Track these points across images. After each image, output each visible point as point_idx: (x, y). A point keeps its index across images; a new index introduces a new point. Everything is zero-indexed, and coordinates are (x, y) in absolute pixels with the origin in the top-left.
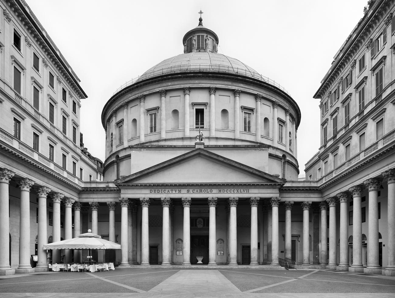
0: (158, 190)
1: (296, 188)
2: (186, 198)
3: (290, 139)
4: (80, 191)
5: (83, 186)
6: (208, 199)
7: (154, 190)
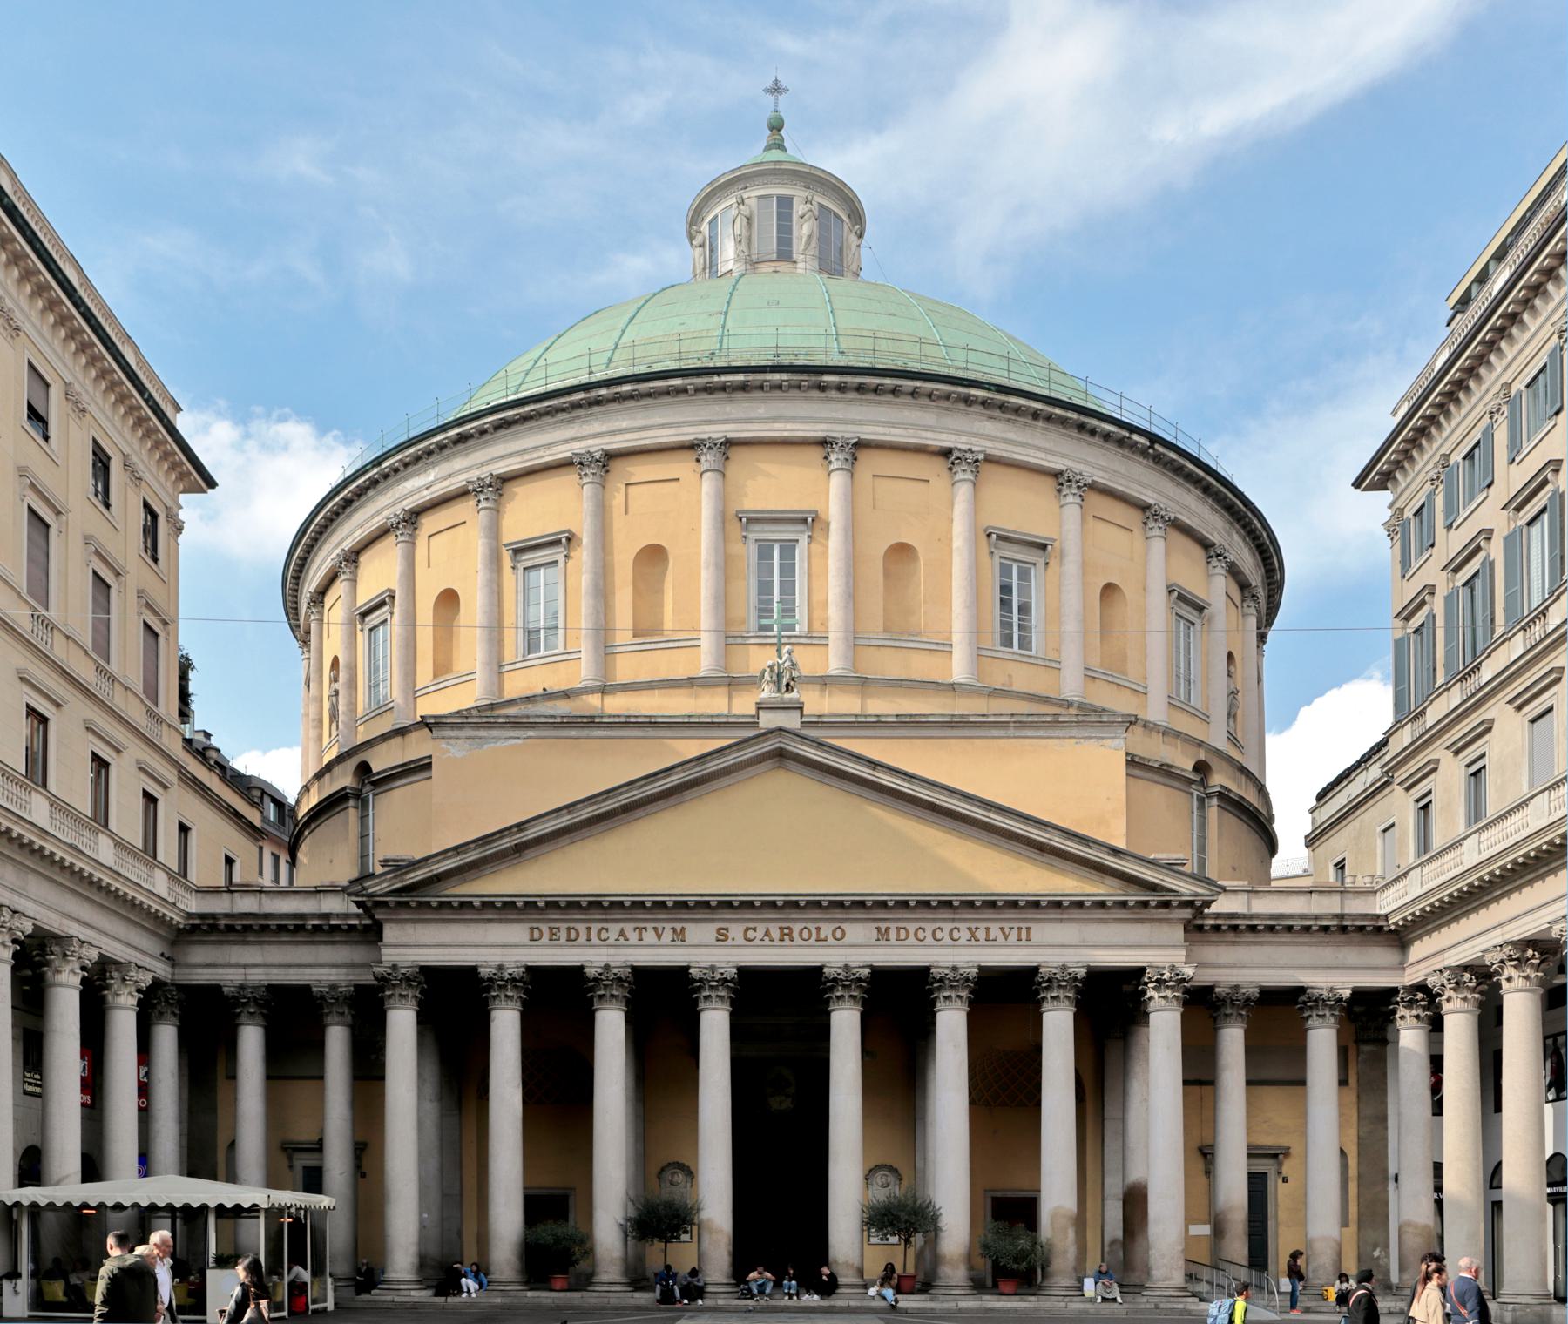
2: (713, 968)
3: (1232, 688)
4: (179, 929)
5: (193, 910)
6: (826, 970)
7: (551, 929)
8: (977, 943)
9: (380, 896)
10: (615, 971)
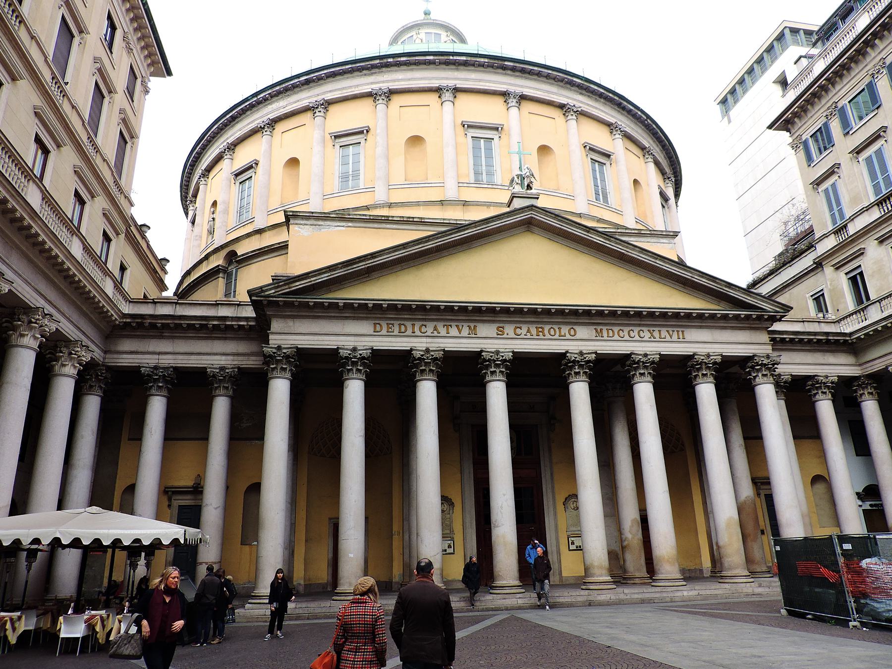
0: (399, 325)
1: (792, 337)
2: (497, 352)
8: (654, 340)
9: (272, 297)
10: (432, 353)
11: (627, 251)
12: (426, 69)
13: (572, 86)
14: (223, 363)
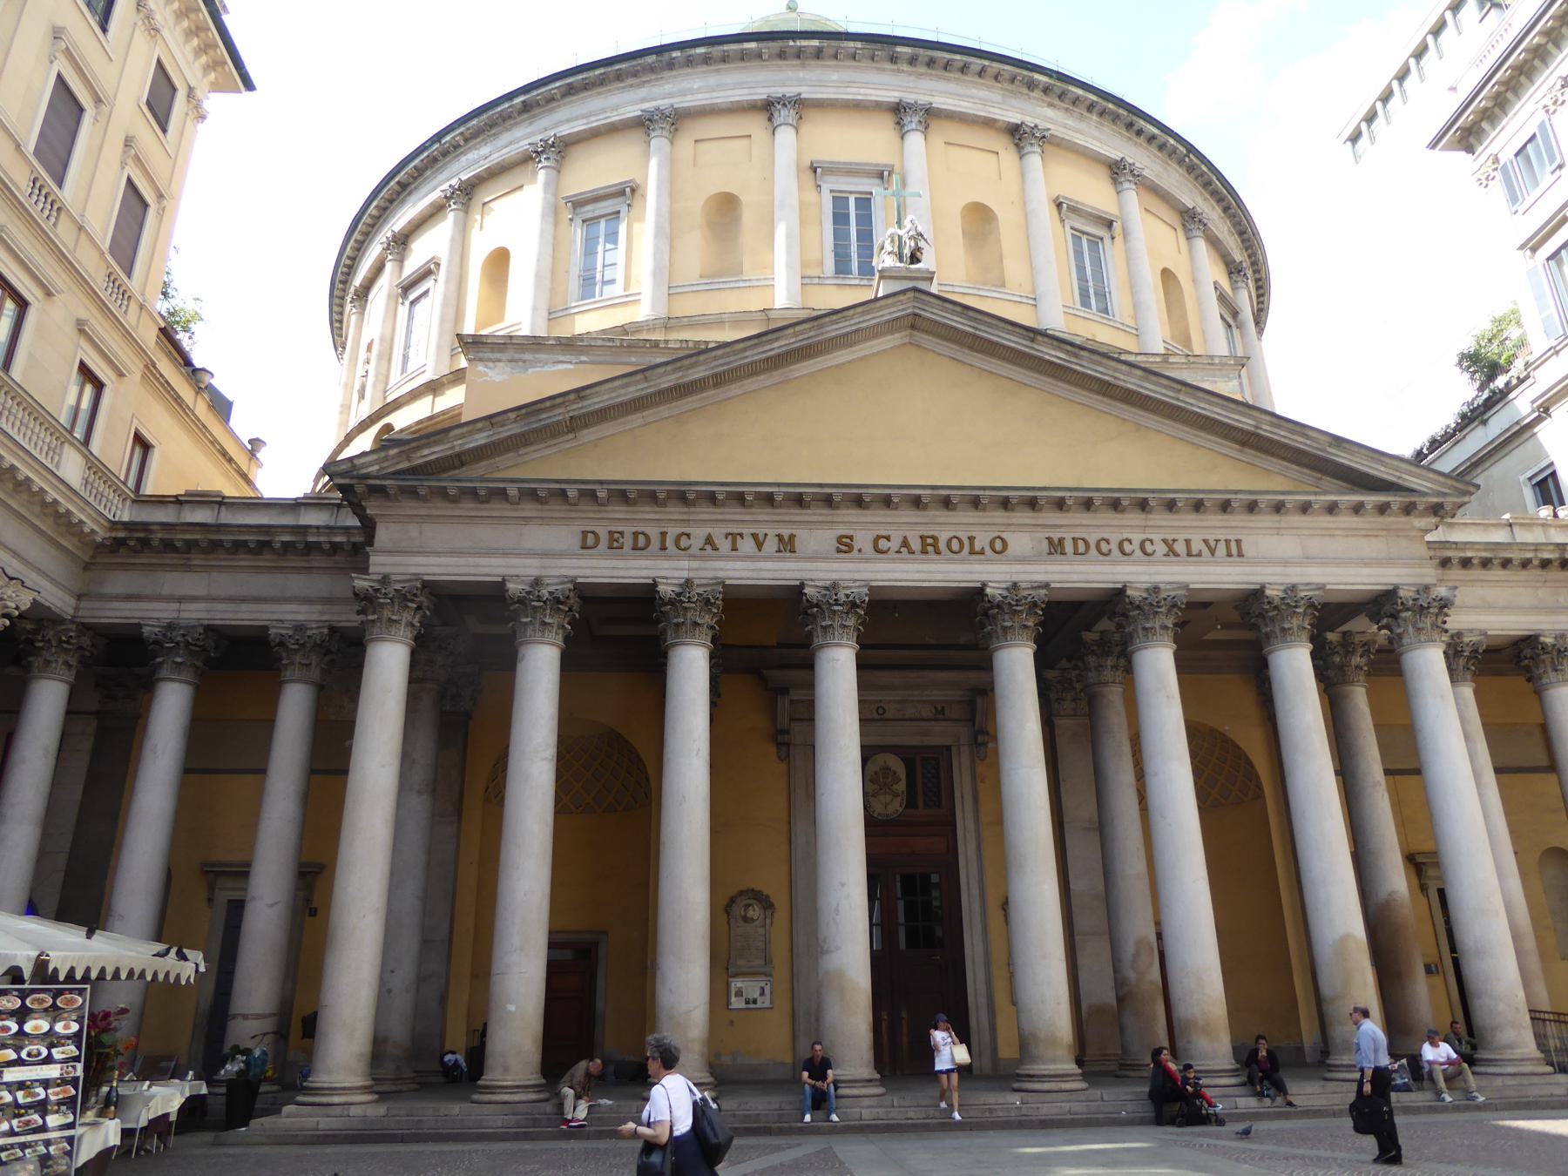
0: (636, 534)
2: (835, 586)
11: (1115, 378)
12: (744, 68)
13: (1033, 91)
14: (300, 617)
